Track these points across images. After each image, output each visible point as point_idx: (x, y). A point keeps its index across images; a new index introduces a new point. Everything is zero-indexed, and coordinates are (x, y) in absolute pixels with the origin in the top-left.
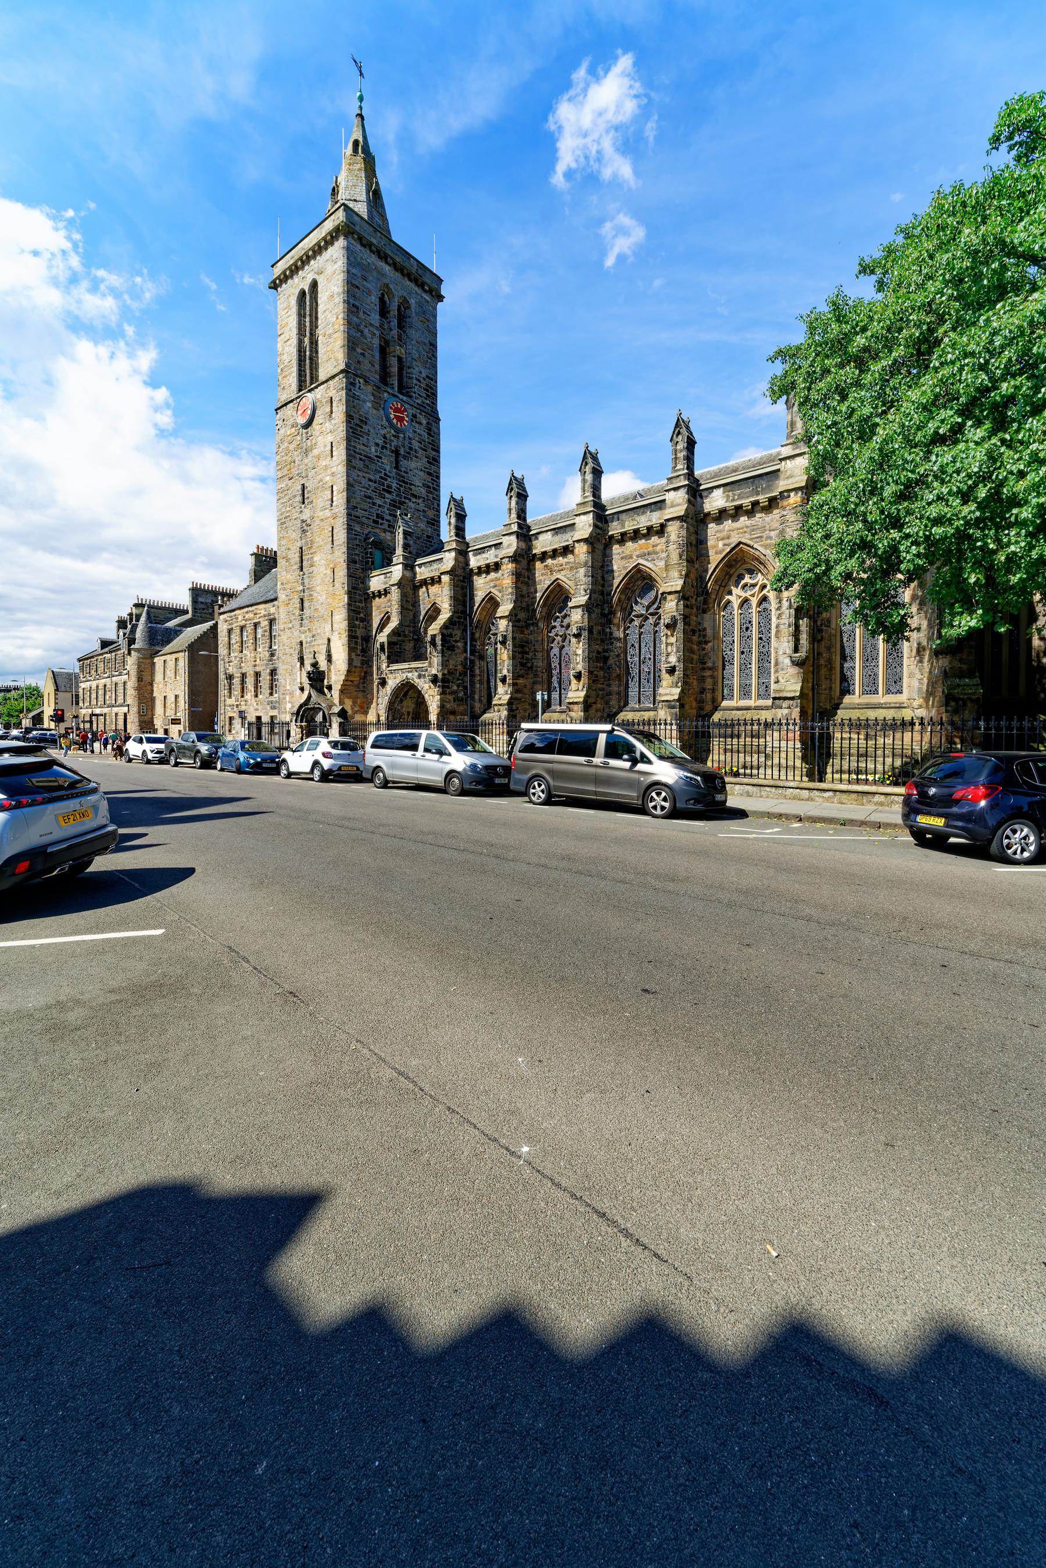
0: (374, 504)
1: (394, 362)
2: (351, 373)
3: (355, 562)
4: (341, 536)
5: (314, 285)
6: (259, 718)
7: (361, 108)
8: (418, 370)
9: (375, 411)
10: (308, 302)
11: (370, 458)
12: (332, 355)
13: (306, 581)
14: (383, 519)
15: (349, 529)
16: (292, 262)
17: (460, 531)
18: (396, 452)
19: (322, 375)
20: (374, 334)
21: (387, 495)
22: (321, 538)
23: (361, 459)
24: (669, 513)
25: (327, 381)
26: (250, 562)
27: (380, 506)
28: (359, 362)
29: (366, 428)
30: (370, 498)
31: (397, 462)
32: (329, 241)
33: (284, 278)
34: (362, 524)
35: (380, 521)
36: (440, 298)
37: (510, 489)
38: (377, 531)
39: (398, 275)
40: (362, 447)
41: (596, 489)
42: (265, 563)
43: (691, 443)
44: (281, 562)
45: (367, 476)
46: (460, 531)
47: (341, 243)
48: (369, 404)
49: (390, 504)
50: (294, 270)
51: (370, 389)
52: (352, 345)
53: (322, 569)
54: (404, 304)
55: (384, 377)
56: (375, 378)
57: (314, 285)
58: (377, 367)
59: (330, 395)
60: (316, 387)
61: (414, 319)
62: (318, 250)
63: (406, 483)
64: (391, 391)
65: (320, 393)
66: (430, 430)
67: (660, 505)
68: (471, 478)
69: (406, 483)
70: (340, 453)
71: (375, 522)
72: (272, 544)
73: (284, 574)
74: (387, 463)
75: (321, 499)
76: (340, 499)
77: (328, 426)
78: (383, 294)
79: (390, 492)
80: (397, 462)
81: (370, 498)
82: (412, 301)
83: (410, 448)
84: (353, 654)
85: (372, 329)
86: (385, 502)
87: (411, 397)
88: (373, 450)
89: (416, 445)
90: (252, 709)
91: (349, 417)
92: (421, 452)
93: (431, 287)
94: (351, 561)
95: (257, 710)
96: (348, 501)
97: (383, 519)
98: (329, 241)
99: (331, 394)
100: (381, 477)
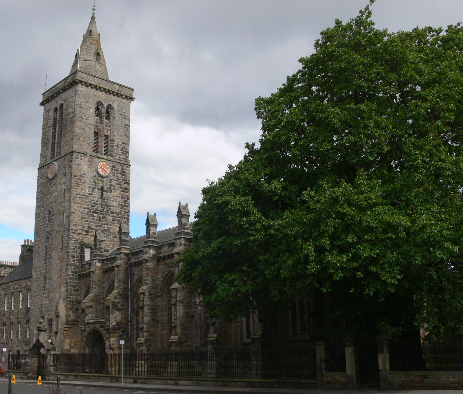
0: (86, 221)
3: (74, 257)
6: (18, 351)
7: (93, 14)
8: (118, 140)
9: (90, 169)
11: (85, 196)
13: (48, 267)
14: (92, 229)
16: (52, 94)
18: (102, 189)
19: (63, 153)
20: (91, 129)
21: (95, 215)
23: (80, 197)
25: (64, 156)
27: (90, 222)
28: (81, 145)
29: (83, 180)
30: (85, 218)
31: (102, 195)
34: (79, 234)
35: (90, 230)
38: (88, 236)
39: (107, 95)
40: (81, 191)
45: (83, 206)
48: (86, 166)
49: (97, 220)
51: (87, 158)
55: (96, 150)
56: (90, 151)
58: (92, 145)
60: (59, 159)
61: (116, 114)
63: (106, 205)
64: (100, 156)
66: (124, 172)
69: (106, 205)
71: (87, 232)
74: (97, 195)
77: (63, 180)
78: (98, 106)
79: (97, 213)
80: (102, 195)
81: (85, 218)
82: (115, 106)
83: (111, 185)
84: (71, 313)
85: (89, 126)
86: (94, 219)
87: (112, 156)
88: (87, 191)
89: (114, 183)
90: (15, 346)
92: (117, 186)
95: (17, 346)
97: (92, 229)
99: (65, 163)
100: (92, 206)
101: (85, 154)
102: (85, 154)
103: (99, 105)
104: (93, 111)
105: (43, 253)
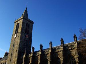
1: (27, 31)
2: (22, 32)
4: (18, 51)
5: (19, 23)
10: (18, 25)
12: (20, 30)
15: (19, 50)
17: (33, 51)
19: (18, 32)
22: (15, 51)
24: (61, 50)
26: (5, 54)
32: (22, 19)
33: (16, 22)
36: (33, 24)
37: (40, 46)
41: (52, 46)
42: (7, 54)
43: (63, 41)
44: (9, 54)
46: (33, 51)
47: (22, 19)
50: (17, 22)
52: (22, 29)
53: (14, 55)
54: (29, 25)
55: (26, 32)
57: (19, 23)
59: (19, 34)
62: (20, 20)
65: (18, 34)
67: (60, 49)
68: (36, 45)
70: (19, 41)
72: (8, 52)
73: (9, 56)
75: (15, 46)
76: (18, 46)
91: (21, 37)
93: (32, 23)
94: (19, 54)
96: (19, 47)
98: (22, 19)
101: (24, 33)
102: (24, 33)
103: (27, 24)
104: (26, 24)
105: (11, 53)
